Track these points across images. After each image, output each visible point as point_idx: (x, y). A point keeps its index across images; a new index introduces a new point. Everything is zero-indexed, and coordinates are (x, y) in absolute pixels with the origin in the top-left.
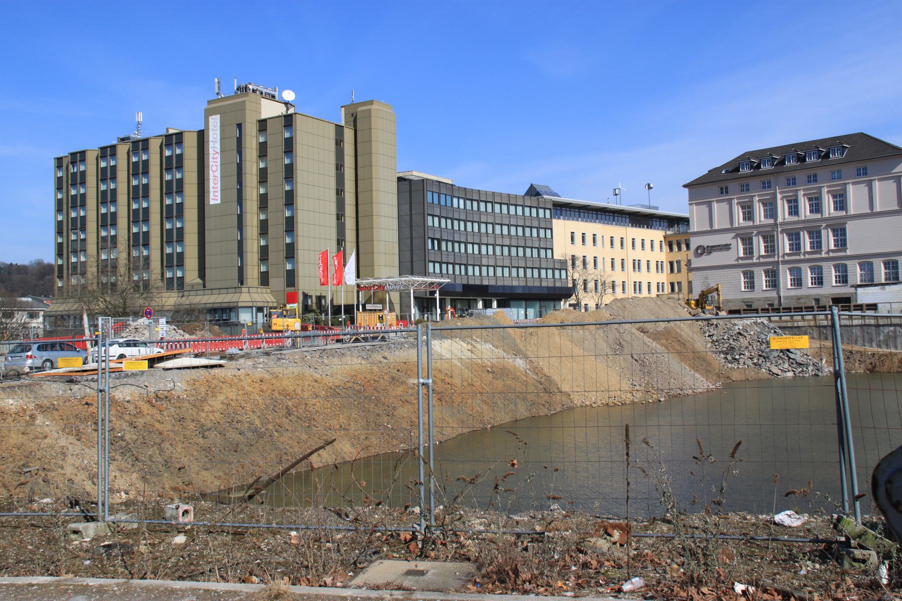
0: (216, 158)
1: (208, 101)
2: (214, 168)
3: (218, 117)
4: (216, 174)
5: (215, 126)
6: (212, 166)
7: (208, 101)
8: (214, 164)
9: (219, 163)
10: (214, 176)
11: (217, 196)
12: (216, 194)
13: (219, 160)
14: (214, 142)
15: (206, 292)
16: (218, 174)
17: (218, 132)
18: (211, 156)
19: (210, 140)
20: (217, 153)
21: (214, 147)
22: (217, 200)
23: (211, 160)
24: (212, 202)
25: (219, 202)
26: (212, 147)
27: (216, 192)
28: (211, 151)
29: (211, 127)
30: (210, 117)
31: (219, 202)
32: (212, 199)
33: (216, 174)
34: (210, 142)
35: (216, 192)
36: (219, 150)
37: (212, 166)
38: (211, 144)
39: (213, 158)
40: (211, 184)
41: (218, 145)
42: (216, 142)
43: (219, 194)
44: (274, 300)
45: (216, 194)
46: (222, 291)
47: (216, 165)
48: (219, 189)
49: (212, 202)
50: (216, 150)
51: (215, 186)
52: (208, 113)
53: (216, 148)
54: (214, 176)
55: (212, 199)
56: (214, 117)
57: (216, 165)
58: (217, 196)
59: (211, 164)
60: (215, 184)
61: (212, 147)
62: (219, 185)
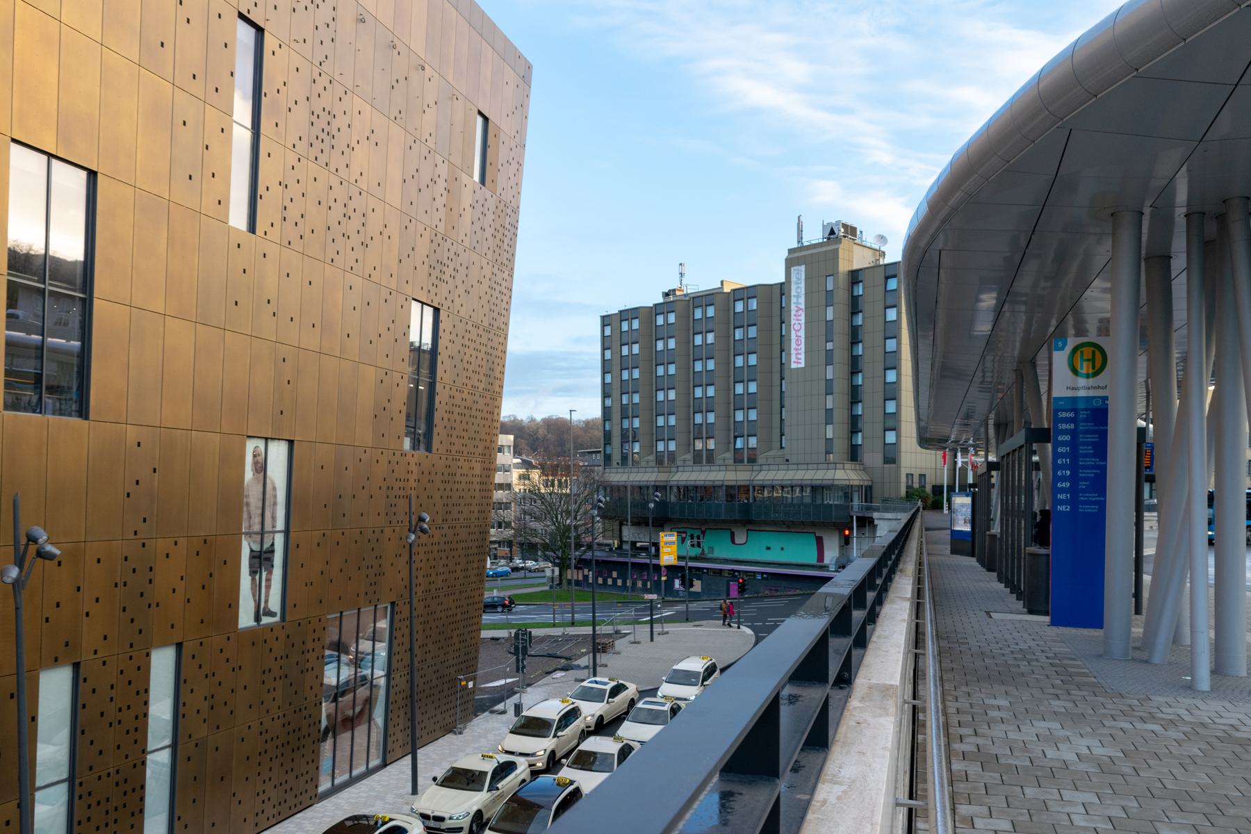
1: (789, 250)
2: (797, 327)
4: (799, 334)
5: (798, 279)
6: (795, 324)
7: (789, 250)
8: (797, 322)
9: (803, 321)
10: (797, 336)
11: (800, 359)
12: (799, 356)
13: (803, 318)
14: (798, 297)
15: (790, 467)
16: (802, 333)
17: (803, 285)
18: (793, 313)
19: (792, 294)
20: (801, 309)
21: (797, 303)
22: (800, 363)
23: (793, 317)
24: (793, 366)
25: (802, 365)
26: (794, 303)
27: (800, 354)
28: (793, 307)
29: (793, 279)
30: (792, 269)
31: (802, 365)
32: (795, 362)
33: (799, 334)
34: (792, 297)
35: (800, 354)
36: (803, 306)
37: (795, 324)
38: (793, 300)
39: (795, 315)
40: (793, 345)
41: (802, 300)
43: (802, 357)
44: (868, 478)
45: (799, 356)
46: (800, 466)
47: (799, 324)
48: (803, 350)
49: (793, 366)
50: (799, 306)
51: (799, 347)
52: (790, 263)
53: (800, 304)
54: (797, 336)
55: (795, 362)
56: (796, 268)
57: (799, 324)
58: (800, 359)
59: (793, 322)
60: (798, 345)
61: (794, 303)
62: (803, 346)
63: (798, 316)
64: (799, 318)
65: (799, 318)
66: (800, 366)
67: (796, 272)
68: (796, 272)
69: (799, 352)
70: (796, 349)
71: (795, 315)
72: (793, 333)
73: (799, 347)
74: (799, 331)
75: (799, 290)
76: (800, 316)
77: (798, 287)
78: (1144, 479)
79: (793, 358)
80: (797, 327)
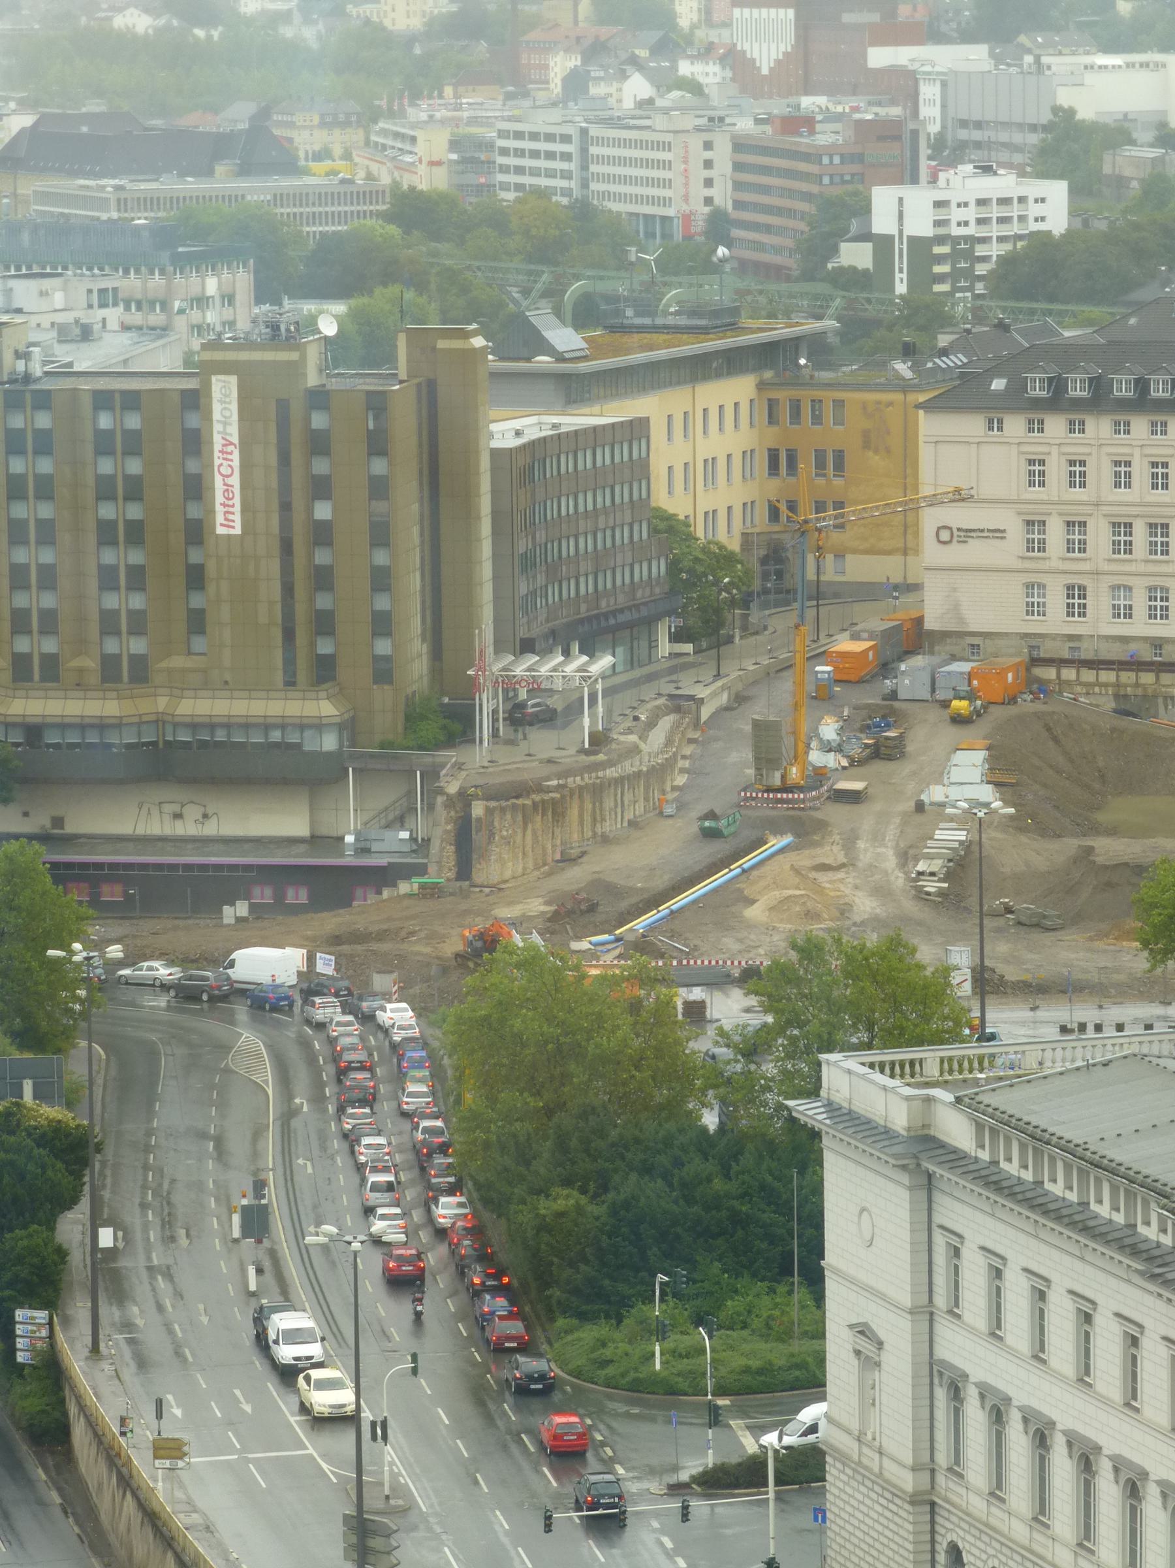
0: (231, 453)
3: (233, 380)
4: (229, 481)
5: (226, 396)
6: (221, 465)
8: (225, 463)
9: (236, 463)
10: (225, 484)
12: (231, 517)
13: (236, 457)
16: (235, 481)
17: (234, 407)
18: (217, 447)
20: (231, 443)
21: (224, 432)
22: (233, 527)
23: (216, 454)
24: (220, 530)
31: (238, 531)
32: (222, 525)
33: (229, 481)
34: (215, 423)
36: (235, 439)
37: (221, 465)
38: (217, 427)
40: (219, 498)
42: (230, 424)
43: (237, 518)
45: (231, 517)
47: (230, 466)
49: (220, 530)
50: (228, 438)
51: (230, 503)
53: (231, 435)
54: (225, 484)
55: (222, 525)
56: (222, 377)
57: (230, 466)
59: (217, 462)
63: (227, 453)
64: (229, 457)
65: (229, 457)
66: (232, 532)
67: (221, 384)
68: (221, 384)
69: (231, 509)
70: (224, 505)
71: (221, 452)
72: (218, 482)
73: (230, 503)
74: (228, 476)
75: (227, 414)
76: (231, 453)
77: (225, 409)
79: (220, 519)
80: (227, 471)
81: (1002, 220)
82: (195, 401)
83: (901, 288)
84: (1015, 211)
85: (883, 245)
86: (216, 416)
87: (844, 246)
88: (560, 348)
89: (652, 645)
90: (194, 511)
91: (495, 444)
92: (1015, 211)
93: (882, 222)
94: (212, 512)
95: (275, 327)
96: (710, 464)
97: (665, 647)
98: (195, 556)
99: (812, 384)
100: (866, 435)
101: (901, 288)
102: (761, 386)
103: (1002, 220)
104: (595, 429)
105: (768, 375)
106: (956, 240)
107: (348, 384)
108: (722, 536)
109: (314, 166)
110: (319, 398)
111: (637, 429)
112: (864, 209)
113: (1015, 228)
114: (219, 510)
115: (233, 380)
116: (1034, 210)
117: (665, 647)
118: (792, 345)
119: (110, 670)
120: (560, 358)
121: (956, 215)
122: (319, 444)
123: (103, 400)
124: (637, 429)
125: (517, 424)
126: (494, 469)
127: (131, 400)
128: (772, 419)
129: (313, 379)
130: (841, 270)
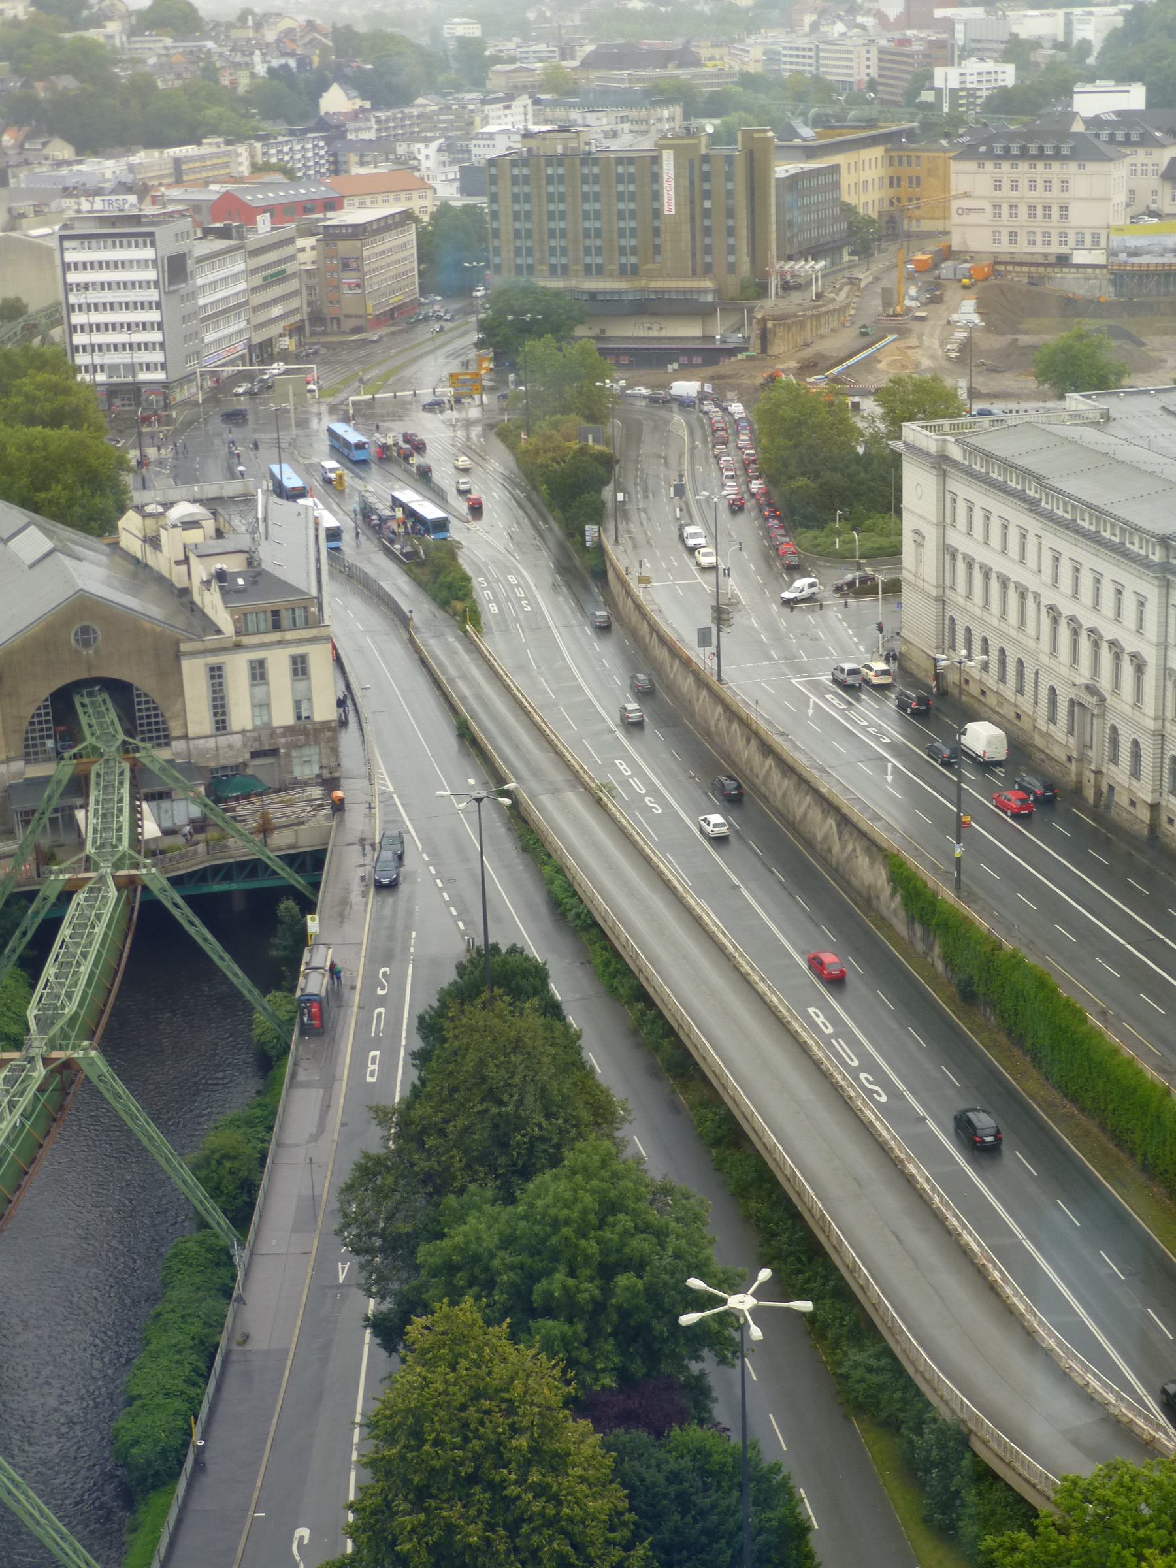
3: (671, 152)
13: (672, 184)
16: (672, 193)
17: (672, 163)
25: (673, 213)
31: (673, 213)
38: (665, 171)
40: (666, 200)
43: (673, 208)
78: (774, 251)
79: (666, 208)
81: (988, 81)
82: (656, 160)
83: (946, 109)
84: (993, 77)
85: (939, 92)
86: (665, 167)
87: (923, 92)
88: (805, 135)
89: (841, 257)
90: (656, 205)
91: (778, 176)
92: (993, 77)
93: (938, 82)
94: (663, 205)
95: (688, 130)
96: (866, 183)
97: (846, 258)
98: (656, 223)
99: (907, 149)
100: (929, 170)
101: (946, 109)
102: (887, 150)
103: (988, 81)
104: (818, 169)
105: (889, 146)
106: (969, 89)
107: (717, 152)
108: (870, 212)
109: (707, 63)
110: (706, 159)
111: (835, 169)
112: (930, 77)
113: (993, 84)
114: (666, 205)
115: (671, 152)
116: (1001, 76)
117: (846, 258)
118: (899, 133)
119: (623, 270)
120: (804, 140)
121: (969, 79)
122: (706, 177)
123: (619, 161)
124: (835, 169)
125: (786, 167)
126: (777, 186)
127: (631, 161)
128: (891, 164)
129: (703, 151)
130: (921, 103)
